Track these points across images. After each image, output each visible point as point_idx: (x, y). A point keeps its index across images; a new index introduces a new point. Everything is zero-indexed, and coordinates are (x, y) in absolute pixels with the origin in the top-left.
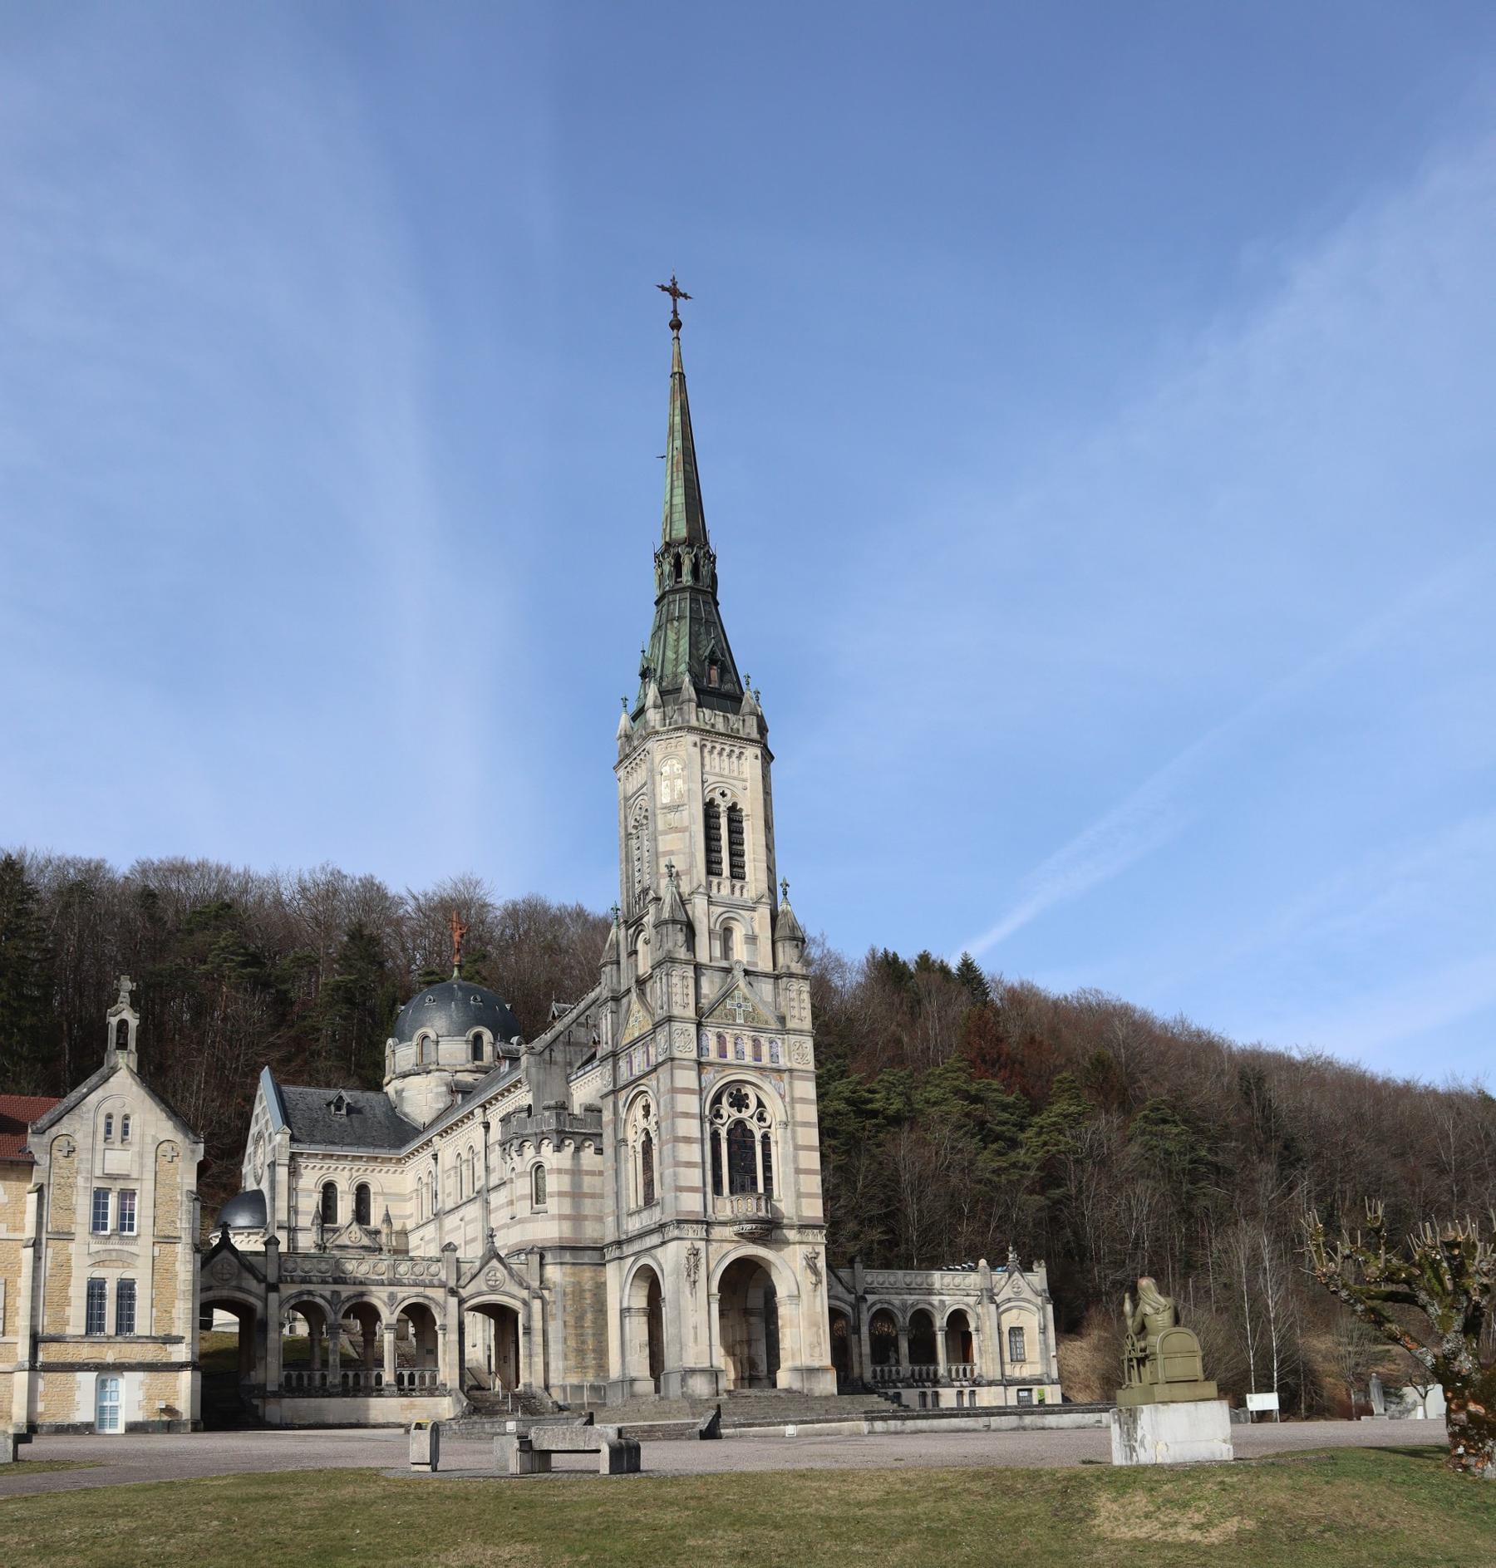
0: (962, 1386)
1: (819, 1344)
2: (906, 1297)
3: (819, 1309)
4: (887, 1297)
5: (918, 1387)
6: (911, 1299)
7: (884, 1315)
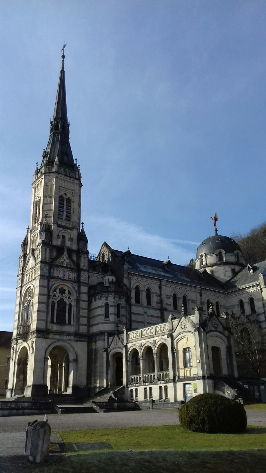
0: (160, 384)
1: (31, 376)
2: (141, 342)
3: (32, 363)
4: (135, 343)
5: (143, 385)
6: (143, 342)
7: (135, 352)
